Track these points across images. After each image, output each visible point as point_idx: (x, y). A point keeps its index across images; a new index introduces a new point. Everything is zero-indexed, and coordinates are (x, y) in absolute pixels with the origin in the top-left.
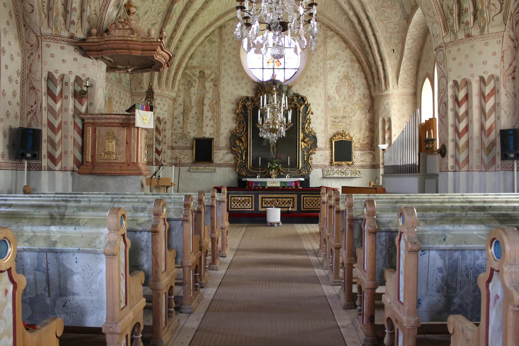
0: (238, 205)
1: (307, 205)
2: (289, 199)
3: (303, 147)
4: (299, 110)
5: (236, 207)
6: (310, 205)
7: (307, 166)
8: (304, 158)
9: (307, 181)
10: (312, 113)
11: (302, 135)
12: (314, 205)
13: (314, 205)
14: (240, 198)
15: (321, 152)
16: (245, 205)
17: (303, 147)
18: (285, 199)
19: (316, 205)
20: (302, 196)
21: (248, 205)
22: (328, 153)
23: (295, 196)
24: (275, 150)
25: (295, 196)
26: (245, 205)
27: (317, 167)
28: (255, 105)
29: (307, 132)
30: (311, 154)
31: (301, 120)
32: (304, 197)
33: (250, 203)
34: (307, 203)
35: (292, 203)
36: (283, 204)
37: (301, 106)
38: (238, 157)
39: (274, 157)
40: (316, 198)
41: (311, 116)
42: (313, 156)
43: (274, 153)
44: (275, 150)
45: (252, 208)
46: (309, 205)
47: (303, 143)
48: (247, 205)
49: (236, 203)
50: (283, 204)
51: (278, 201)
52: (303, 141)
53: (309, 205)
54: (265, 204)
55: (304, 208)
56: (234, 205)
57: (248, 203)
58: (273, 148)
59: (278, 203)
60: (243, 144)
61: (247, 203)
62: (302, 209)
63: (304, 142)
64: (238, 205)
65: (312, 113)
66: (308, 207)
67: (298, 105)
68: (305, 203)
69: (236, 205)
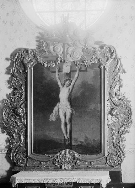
3: (111, 122)
4: (104, 68)
8: (113, 139)
10: (124, 72)
11: (109, 105)
24: (68, 127)
28: (37, 60)
29: (116, 99)
30: (123, 132)
31: (107, 82)
37: (107, 60)
38: (14, 138)
39: (67, 137)
41: (123, 76)
43: (67, 133)
44: (68, 127)
47: (110, 116)
52: (111, 113)
58: (66, 125)
60: (20, 119)
63: (112, 115)
65: (124, 72)
67: (103, 59)
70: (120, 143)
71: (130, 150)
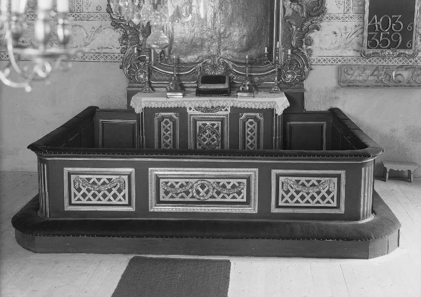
0: (90, 195)
1: (287, 197)
2: (233, 182)
5: (84, 201)
6: (297, 197)
7: (300, 62)
9: (296, 99)
12: (308, 198)
13: (308, 198)
14: (94, 178)
15: (336, 25)
16: (110, 196)
17: (289, 12)
18: (223, 182)
19: (313, 198)
20: (274, 172)
21: (120, 196)
22: (352, 24)
23: (253, 172)
25: (253, 172)
26: (110, 196)
27: (324, 61)
30: (308, 30)
32: (278, 176)
33: (126, 191)
34: (287, 192)
35: (244, 192)
36: (218, 193)
40: (314, 180)
42: (313, 35)
45: (130, 204)
46: (292, 197)
48: (115, 196)
49: (84, 190)
50: (218, 193)
51: (203, 187)
53: (292, 197)
54: (167, 193)
55: (277, 206)
56: (79, 195)
57: (120, 191)
59: (202, 192)
61: (114, 191)
62: (274, 210)
64: (90, 195)
66: (292, 203)
68: (281, 192)
69: (84, 195)
70: (304, 46)
71: (320, 58)
